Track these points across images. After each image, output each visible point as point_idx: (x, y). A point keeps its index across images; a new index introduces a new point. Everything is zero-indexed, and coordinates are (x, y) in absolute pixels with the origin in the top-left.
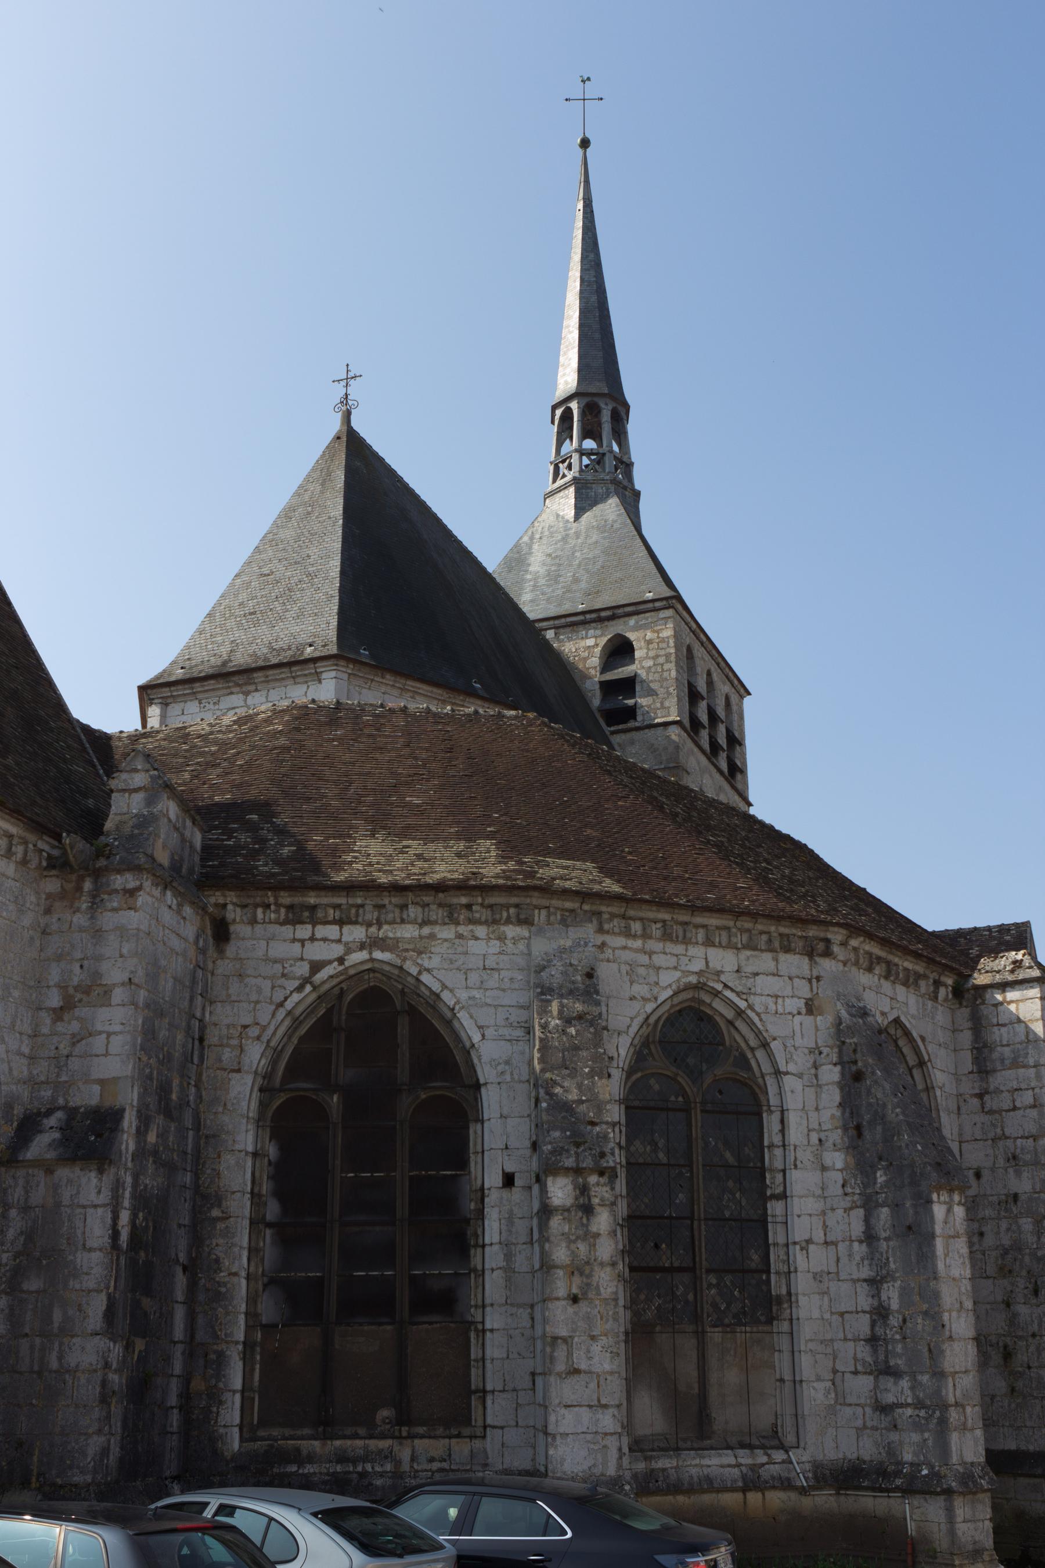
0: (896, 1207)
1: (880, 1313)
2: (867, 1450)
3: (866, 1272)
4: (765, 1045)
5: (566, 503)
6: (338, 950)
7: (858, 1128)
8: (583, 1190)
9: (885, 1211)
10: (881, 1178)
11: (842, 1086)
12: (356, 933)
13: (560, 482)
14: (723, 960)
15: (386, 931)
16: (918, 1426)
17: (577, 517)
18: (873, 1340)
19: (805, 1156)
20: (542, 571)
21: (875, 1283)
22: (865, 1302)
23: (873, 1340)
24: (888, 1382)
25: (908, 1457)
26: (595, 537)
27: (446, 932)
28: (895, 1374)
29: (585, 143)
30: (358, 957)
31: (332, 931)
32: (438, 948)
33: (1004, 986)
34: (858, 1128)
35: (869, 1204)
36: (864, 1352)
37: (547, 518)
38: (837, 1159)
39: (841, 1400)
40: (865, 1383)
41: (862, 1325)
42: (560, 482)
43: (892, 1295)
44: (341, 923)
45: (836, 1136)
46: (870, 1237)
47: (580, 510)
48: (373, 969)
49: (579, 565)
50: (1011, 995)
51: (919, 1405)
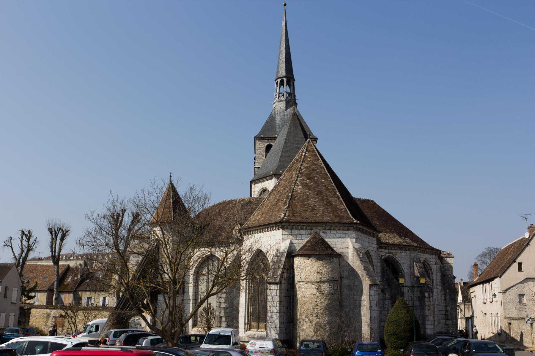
0: (450, 296)
1: (447, 311)
2: (443, 330)
3: (444, 305)
4: (431, 269)
5: (283, 105)
6: (384, 254)
7: (444, 284)
8: (429, 294)
9: (448, 296)
10: (448, 291)
11: (441, 276)
12: (387, 251)
13: (280, 99)
14: (428, 256)
15: (391, 251)
16: (452, 327)
17: (286, 110)
18: (445, 315)
19: (435, 287)
20: (280, 123)
21: (446, 306)
22: (444, 309)
23: (445, 315)
24: (448, 321)
25: (450, 331)
27: (399, 252)
28: (449, 320)
29: (285, 5)
30: (387, 255)
31: (383, 250)
32: (398, 254)
33: (447, 257)
34: (444, 284)
35: (445, 295)
36: (443, 316)
37: (278, 108)
38: (440, 288)
39: (439, 323)
40: (443, 321)
41: (444, 312)
42: (280, 99)
43: (449, 308)
44: (385, 249)
45: (440, 284)
46: (445, 300)
47: (287, 108)
48: (388, 257)
50: (448, 259)
51: (453, 324)
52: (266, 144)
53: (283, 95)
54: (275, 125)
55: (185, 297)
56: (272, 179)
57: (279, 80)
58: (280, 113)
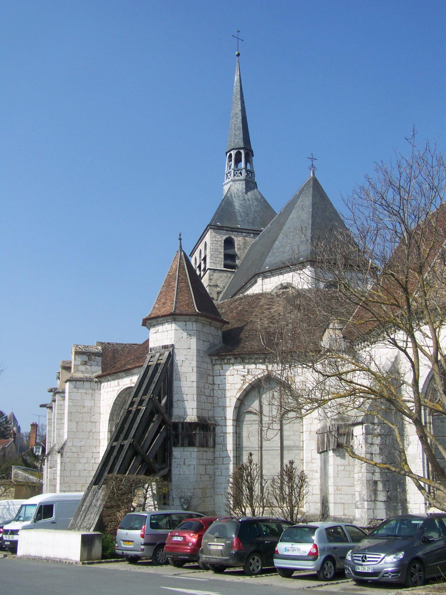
13: (236, 178)
17: (246, 193)
20: (241, 210)
26: (256, 203)
42: (236, 178)
49: (254, 212)
52: (225, 237)
53: (241, 173)
54: (234, 212)
55: (217, 454)
56: (304, 267)
57: (233, 153)
58: (239, 196)
